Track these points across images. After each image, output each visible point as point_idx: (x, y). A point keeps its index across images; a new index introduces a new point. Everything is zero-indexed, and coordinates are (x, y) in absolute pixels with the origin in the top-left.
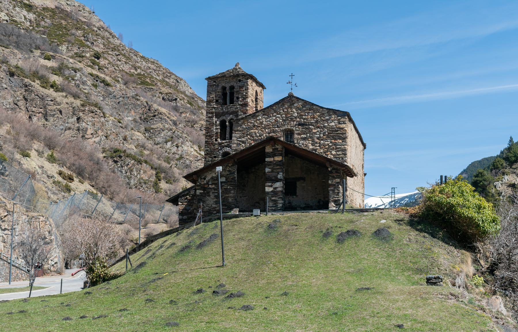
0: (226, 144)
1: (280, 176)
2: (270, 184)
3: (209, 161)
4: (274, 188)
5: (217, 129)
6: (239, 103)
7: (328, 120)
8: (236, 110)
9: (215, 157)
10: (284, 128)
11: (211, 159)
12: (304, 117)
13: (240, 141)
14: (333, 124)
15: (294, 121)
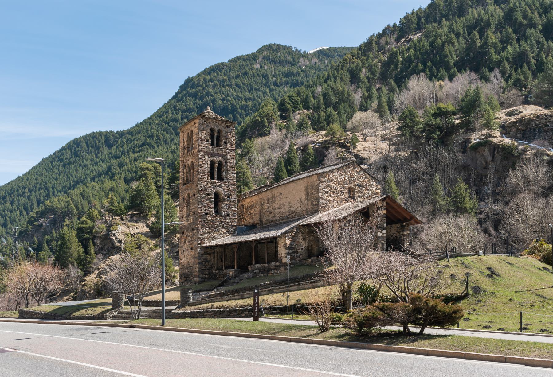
0: (218, 184)
1: (385, 225)
2: (380, 231)
3: (203, 198)
4: (383, 234)
5: (208, 168)
6: (228, 148)
7: (371, 185)
8: (225, 153)
9: (208, 195)
10: (349, 186)
11: (205, 196)
12: (360, 180)
13: (324, 191)
14: (374, 189)
15: (355, 182)
